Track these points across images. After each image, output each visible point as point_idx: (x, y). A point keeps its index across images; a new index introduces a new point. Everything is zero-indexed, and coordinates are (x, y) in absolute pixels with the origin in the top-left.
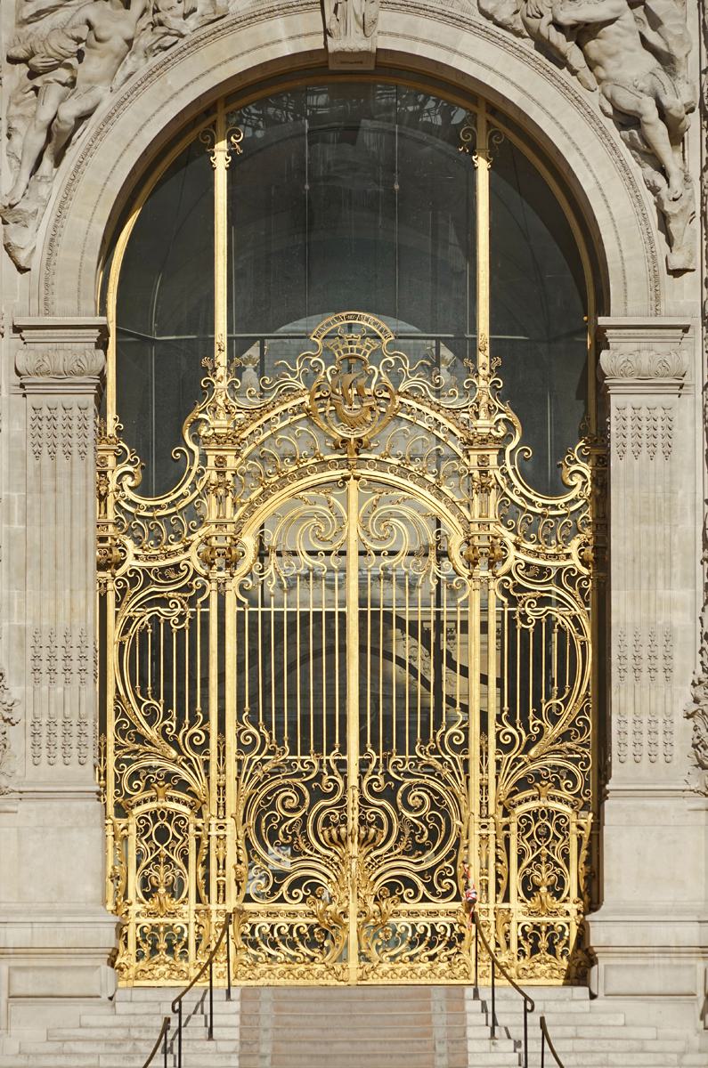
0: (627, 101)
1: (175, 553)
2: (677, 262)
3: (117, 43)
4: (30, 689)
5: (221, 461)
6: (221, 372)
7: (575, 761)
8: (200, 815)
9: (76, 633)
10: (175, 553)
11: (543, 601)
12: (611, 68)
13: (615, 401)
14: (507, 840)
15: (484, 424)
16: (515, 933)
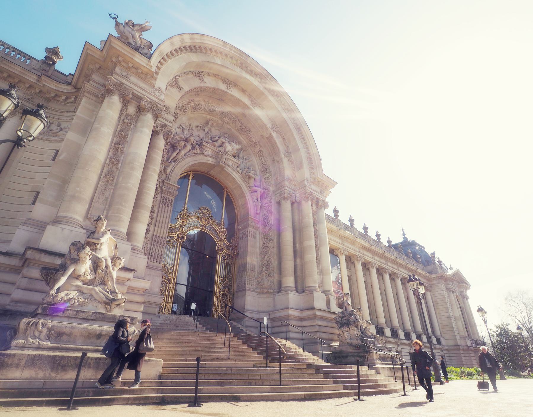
1: (173, 235)
2: (258, 212)
4: (152, 246)
5: (183, 222)
6: (186, 208)
7: (230, 286)
8: (169, 283)
9: (163, 238)
10: (173, 235)
13: (249, 228)
14: (219, 297)
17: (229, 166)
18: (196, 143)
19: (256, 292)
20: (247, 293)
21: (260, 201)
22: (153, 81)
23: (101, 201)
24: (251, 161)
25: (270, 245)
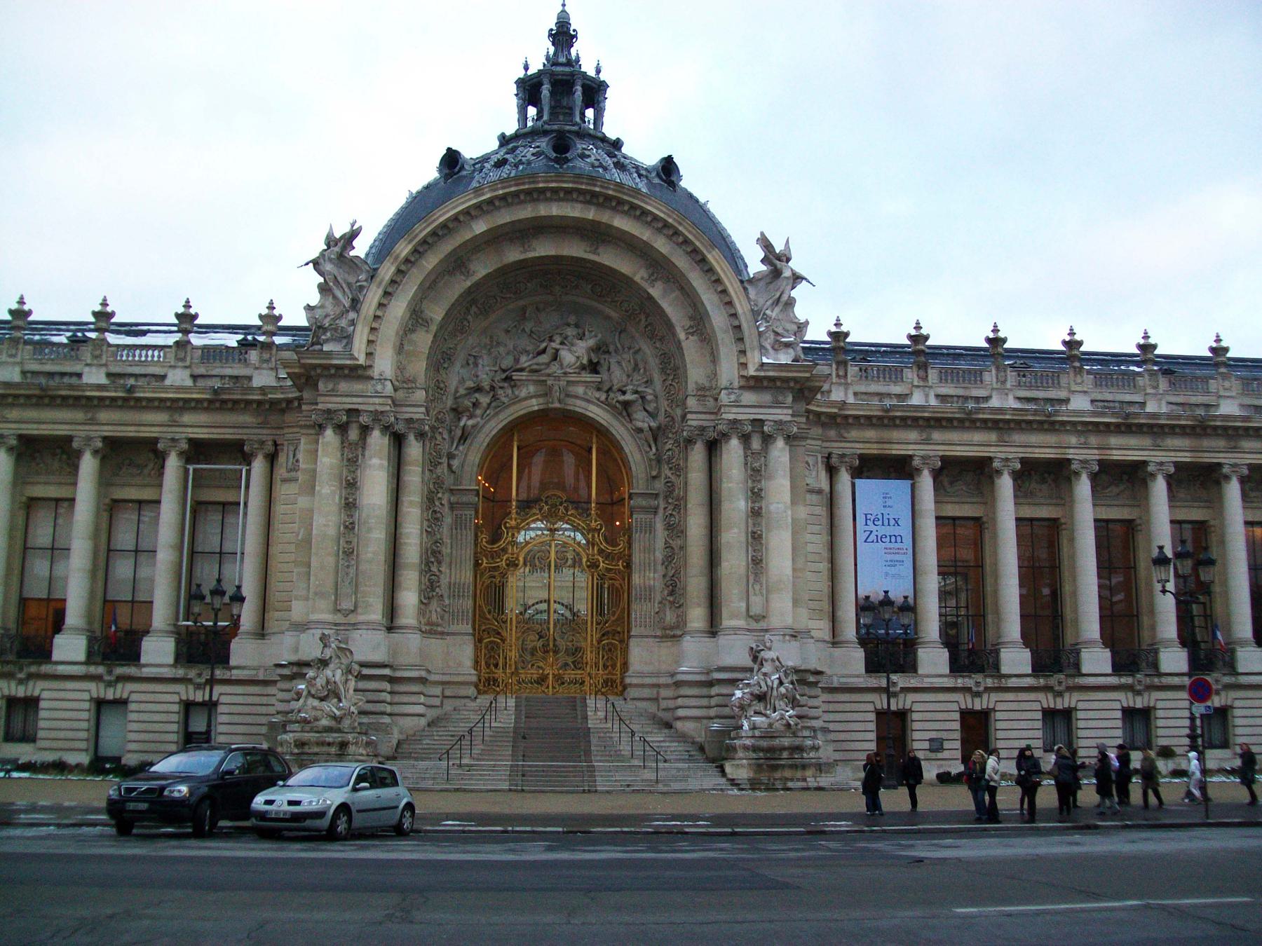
0: (640, 424)
2: (654, 473)
3: (485, 405)
11: (611, 579)
12: (635, 416)
13: (635, 516)
15: (593, 524)
16: (601, 681)
17: (577, 397)
18: (504, 376)
19: (655, 637)
20: (633, 642)
21: (654, 449)
22: (370, 373)
23: (347, 583)
24: (640, 349)
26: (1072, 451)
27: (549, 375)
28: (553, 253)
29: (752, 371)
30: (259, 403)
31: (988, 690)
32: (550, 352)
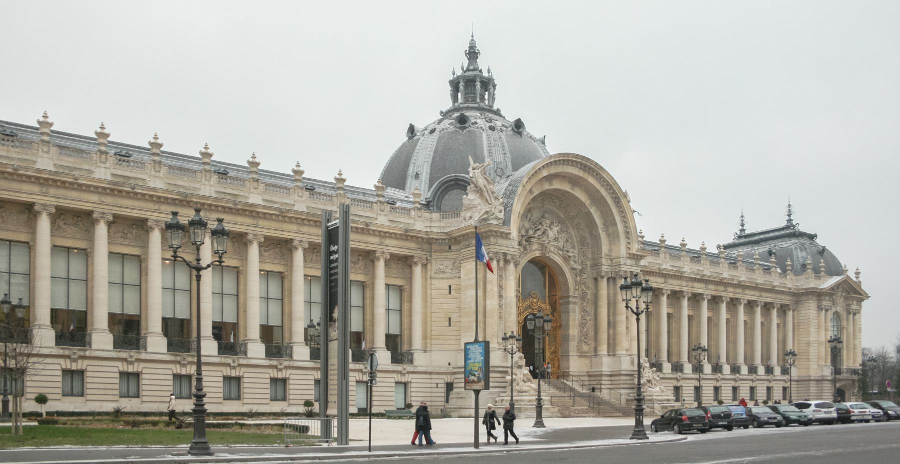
0: (575, 266)
25: (588, 318)
26: (684, 288)
27: (544, 241)
28: (559, 188)
29: (634, 252)
30: (422, 238)
31: (409, 372)
32: (543, 230)
